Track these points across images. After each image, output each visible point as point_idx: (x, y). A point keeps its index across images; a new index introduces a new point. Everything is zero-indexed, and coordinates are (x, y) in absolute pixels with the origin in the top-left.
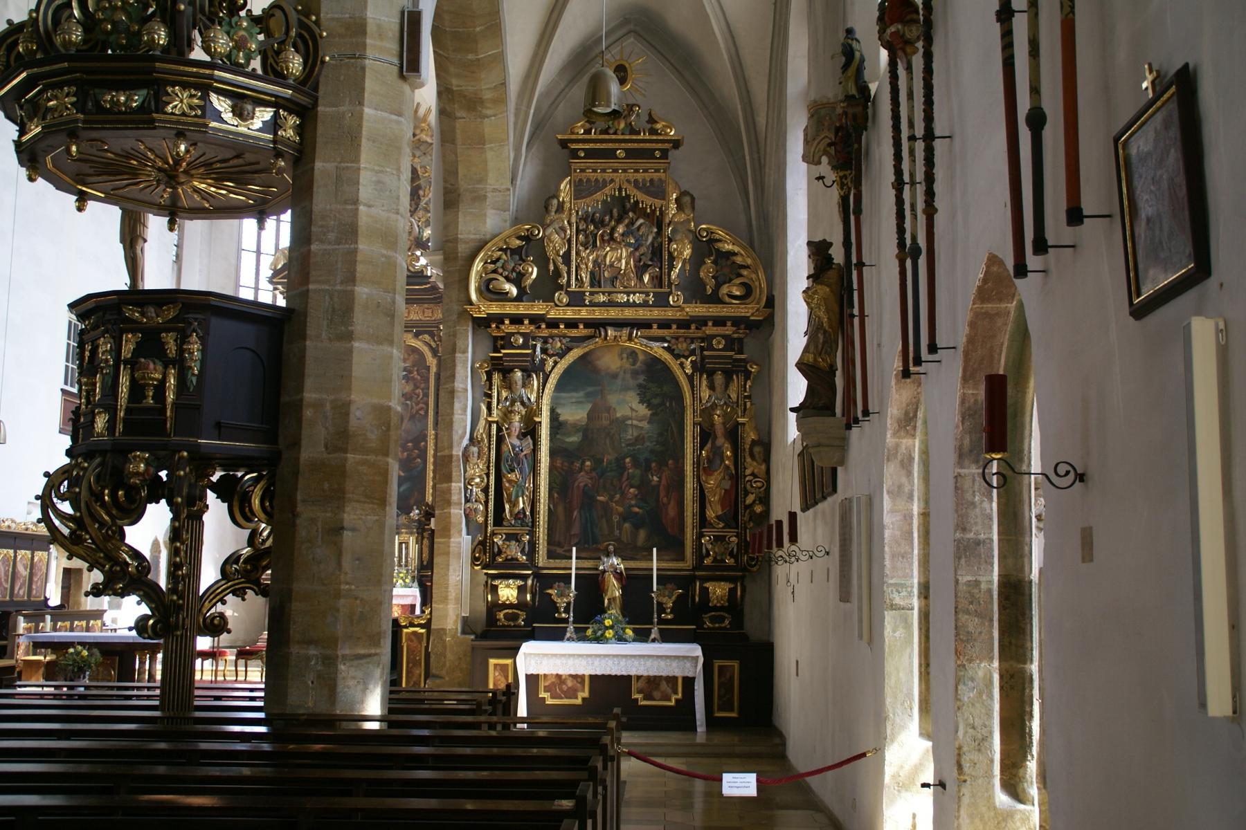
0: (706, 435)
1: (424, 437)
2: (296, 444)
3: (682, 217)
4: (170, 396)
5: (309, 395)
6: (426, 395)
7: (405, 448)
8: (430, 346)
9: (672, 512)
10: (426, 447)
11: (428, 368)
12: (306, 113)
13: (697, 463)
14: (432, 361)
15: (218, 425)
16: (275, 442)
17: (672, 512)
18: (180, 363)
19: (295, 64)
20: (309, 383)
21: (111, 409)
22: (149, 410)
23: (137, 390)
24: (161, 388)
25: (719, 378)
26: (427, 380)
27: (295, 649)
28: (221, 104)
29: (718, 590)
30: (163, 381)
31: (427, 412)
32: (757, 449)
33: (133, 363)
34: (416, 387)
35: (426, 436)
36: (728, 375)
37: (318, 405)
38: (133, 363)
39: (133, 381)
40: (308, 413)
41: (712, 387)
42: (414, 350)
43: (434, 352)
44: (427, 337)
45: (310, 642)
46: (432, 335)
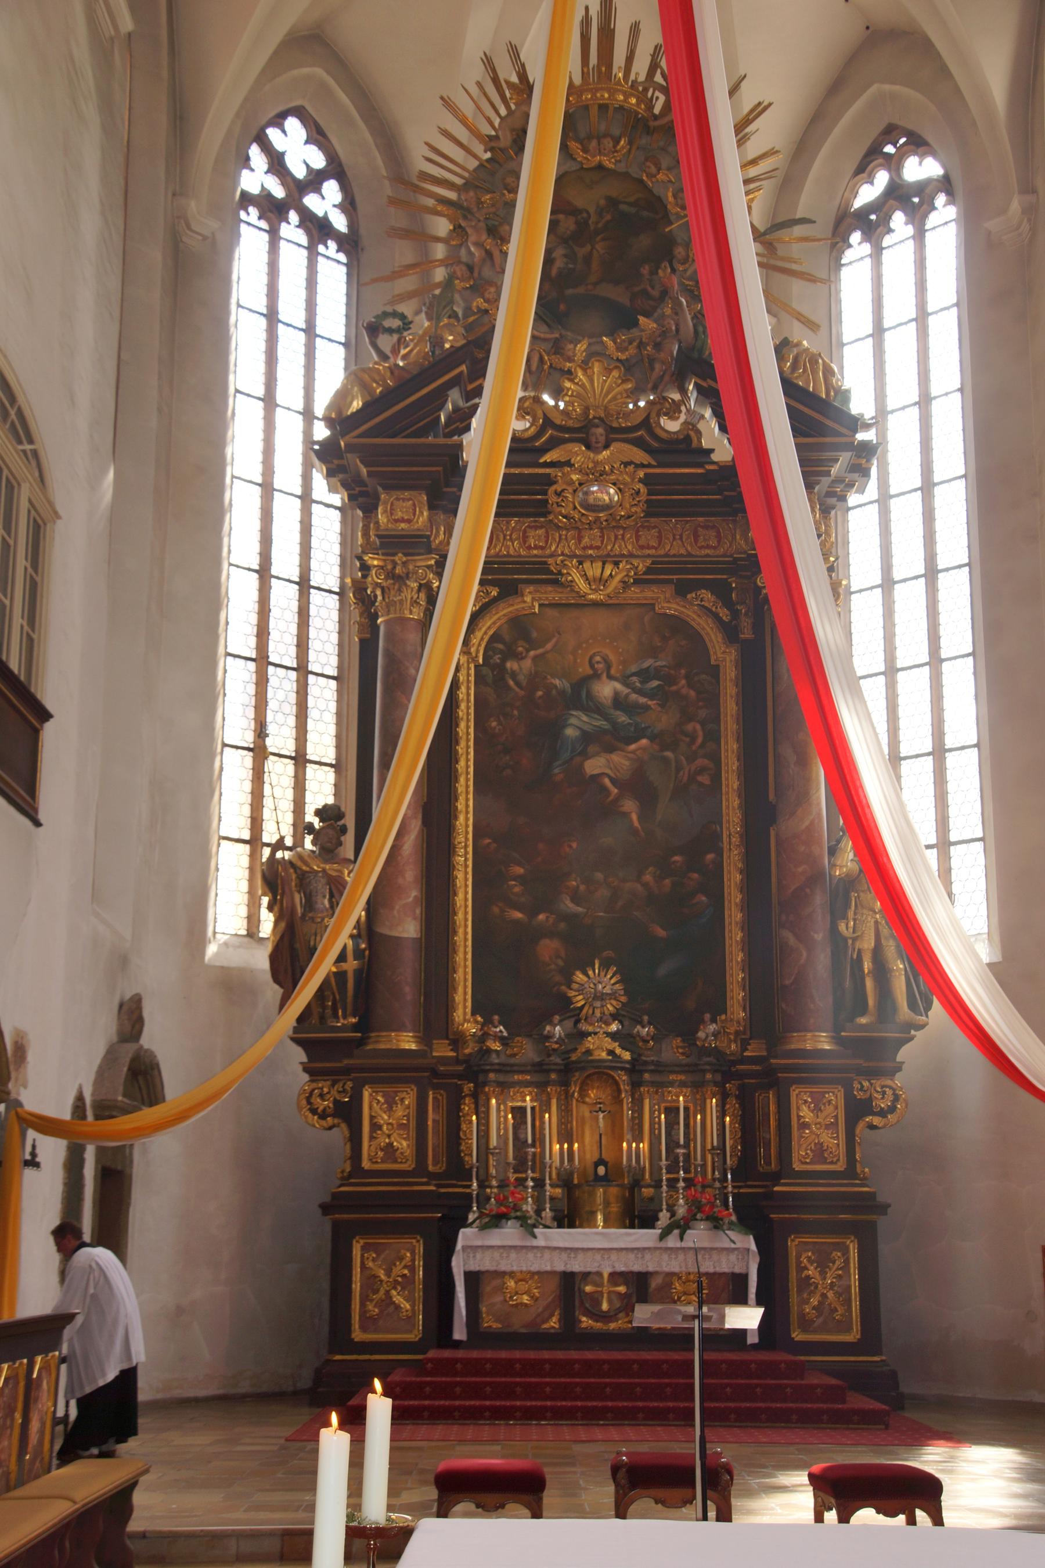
6: (714, 736)
8: (716, 616)
10: (719, 866)
11: (715, 672)
14: (725, 656)
26: (712, 700)
31: (716, 778)
35: (717, 837)
42: (677, 626)
43: (731, 633)
44: (706, 595)
46: (722, 591)
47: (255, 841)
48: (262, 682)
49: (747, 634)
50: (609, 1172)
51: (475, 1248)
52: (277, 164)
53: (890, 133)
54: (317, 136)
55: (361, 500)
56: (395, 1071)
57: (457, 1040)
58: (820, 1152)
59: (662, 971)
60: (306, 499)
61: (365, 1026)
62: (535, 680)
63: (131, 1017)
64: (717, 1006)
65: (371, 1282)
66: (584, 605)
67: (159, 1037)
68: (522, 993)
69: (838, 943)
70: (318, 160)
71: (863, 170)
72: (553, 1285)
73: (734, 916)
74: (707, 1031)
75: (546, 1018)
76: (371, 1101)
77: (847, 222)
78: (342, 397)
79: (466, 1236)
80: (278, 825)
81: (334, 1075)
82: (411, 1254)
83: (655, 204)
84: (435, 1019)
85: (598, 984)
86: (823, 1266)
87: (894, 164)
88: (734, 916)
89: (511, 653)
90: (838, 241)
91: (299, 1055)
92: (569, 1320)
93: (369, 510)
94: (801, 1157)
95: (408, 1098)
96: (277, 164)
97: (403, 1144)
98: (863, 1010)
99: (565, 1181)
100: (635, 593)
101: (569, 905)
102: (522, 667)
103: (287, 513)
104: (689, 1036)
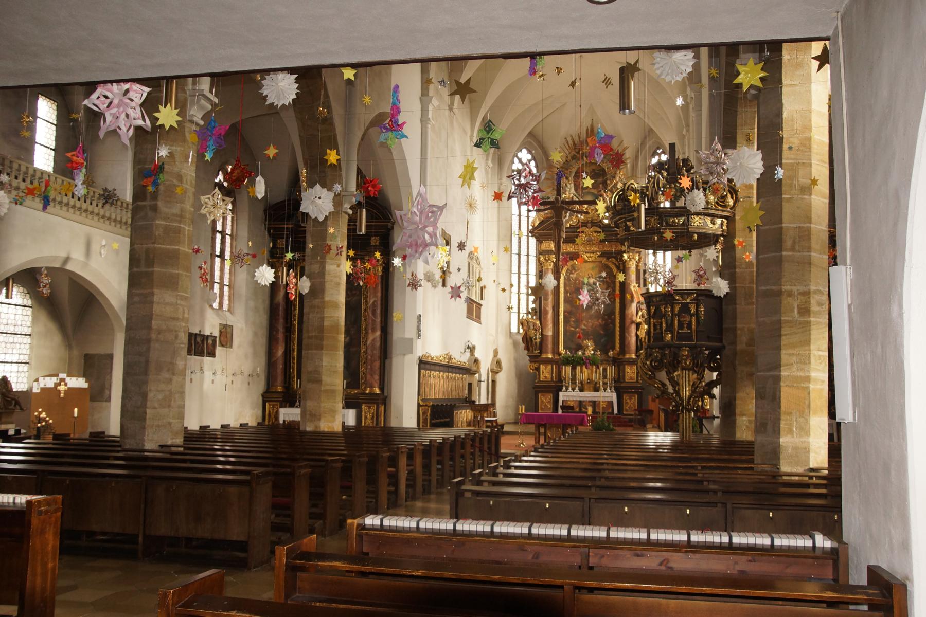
1: (613, 313)
2: (734, 343)
4: (694, 327)
5: (739, 326)
7: (603, 319)
12: (731, 220)
15: (708, 337)
16: (721, 341)
18: (697, 313)
19: (731, 202)
20: (738, 321)
21: (672, 333)
23: (681, 326)
24: (690, 323)
27: (738, 418)
28: (708, 220)
30: (690, 322)
38: (679, 315)
39: (679, 321)
40: (739, 332)
45: (743, 415)
46: (617, 259)
47: (519, 313)
48: (519, 278)
51: (562, 396)
52: (520, 161)
53: (659, 148)
54: (529, 152)
55: (539, 241)
56: (548, 362)
57: (560, 354)
58: (631, 378)
59: (603, 340)
60: (528, 236)
61: (541, 353)
62: (576, 279)
63: (496, 352)
64: (613, 348)
65: (542, 402)
66: (586, 262)
67: (500, 356)
68: (574, 344)
70: (529, 157)
71: (653, 155)
73: (617, 329)
74: (611, 353)
75: (578, 350)
76: (542, 367)
78: (534, 222)
79: (561, 394)
80: (523, 309)
81: (535, 362)
82: (550, 397)
83: (603, 170)
84: (556, 351)
85: (589, 344)
86: (630, 399)
87: (659, 155)
88: (617, 329)
89: (571, 273)
91: (528, 358)
92: (580, 409)
93: (541, 242)
94: (627, 379)
95: (550, 367)
96: (520, 161)
99: (581, 382)
100: (598, 259)
101: (583, 327)
102: (574, 276)
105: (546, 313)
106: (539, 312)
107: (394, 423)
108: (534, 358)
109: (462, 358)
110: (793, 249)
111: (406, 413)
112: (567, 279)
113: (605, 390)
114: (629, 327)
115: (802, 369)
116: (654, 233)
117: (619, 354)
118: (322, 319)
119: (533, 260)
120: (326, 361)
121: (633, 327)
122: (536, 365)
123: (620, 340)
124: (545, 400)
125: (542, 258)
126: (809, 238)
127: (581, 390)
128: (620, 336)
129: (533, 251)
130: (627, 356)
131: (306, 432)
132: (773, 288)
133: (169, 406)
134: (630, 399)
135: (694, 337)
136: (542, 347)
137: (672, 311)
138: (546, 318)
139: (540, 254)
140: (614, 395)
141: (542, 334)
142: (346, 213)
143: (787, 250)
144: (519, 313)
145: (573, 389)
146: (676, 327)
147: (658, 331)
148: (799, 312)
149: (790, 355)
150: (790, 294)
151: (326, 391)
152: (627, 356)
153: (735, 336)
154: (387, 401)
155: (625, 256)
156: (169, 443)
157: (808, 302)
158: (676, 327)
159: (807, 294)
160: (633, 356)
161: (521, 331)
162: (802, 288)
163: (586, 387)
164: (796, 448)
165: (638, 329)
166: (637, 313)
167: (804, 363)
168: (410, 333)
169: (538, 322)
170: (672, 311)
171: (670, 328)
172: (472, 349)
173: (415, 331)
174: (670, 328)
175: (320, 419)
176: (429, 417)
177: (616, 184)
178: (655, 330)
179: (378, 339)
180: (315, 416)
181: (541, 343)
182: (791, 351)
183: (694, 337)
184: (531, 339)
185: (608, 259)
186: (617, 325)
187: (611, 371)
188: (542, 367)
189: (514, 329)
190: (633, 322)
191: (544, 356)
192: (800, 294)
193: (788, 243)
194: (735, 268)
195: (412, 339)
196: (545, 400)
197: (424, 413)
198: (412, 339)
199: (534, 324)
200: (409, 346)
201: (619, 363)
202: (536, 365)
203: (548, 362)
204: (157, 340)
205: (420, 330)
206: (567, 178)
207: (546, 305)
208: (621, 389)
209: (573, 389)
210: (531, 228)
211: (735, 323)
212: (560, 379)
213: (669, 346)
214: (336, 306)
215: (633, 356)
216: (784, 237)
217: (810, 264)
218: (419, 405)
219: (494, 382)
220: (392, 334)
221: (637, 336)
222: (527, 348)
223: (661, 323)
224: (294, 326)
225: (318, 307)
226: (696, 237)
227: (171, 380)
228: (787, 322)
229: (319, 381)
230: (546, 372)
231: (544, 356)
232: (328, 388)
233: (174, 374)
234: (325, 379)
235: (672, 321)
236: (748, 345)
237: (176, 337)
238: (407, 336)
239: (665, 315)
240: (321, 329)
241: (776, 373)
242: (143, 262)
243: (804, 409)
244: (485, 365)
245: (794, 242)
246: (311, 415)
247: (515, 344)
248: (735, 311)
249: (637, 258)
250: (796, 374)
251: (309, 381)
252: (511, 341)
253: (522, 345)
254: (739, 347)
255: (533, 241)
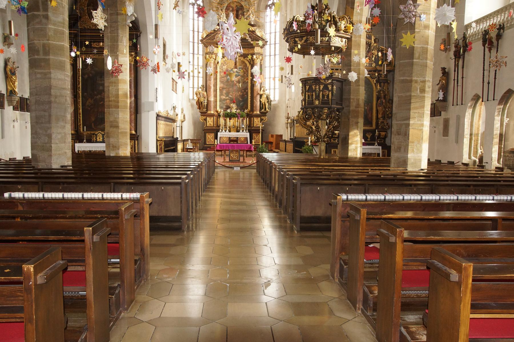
0: (378, 98)
1: (247, 88)
2: (349, 106)
3: (375, 45)
4: (330, 97)
5: (352, 97)
7: (242, 92)
9: (370, 116)
12: (349, 40)
13: (377, 104)
15: (337, 103)
17: (370, 116)
20: (351, 94)
21: (319, 100)
22: (326, 100)
23: (323, 96)
24: (328, 96)
25: (382, 84)
29: (383, 134)
30: (329, 94)
32: (390, 101)
33: (322, 91)
34: (244, 73)
36: (384, 83)
37: (353, 99)
38: (322, 91)
39: (322, 94)
40: (352, 100)
41: (380, 86)
43: (250, 63)
47: (193, 88)
49: (252, 62)
50: (234, 126)
51: (219, 134)
57: (217, 112)
60: (198, 43)
61: (207, 110)
64: (247, 108)
65: (209, 138)
69: (260, 101)
72: (228, 139)
74: (246, 111)
76: (208, 119)
77: (267, 6)
79: (219, 133)
80: (196, 86)
83: (242, 6)
85: (234, 106)
86: (257, 136)
90: (266, 8)
93: (207, 47)
95: (212, 118)
97: (212, 124)
98: (263, 109)
99: (229, 127)
101: (230, 96)
103: (196, 45)
104: (244, 111)
105: (210, 88)
106: (206, 87)
107: (144, 151)
108: (203, 114)
109: (171, 114)
110: (419, 58)
111: (150, 145)
112: (221, 67)
113: (243, 131)
114: (256, 96)
115: (420, 120)
116: (312, 46)
117: (250, 112)
118: (118, 90)
119: (201, 58)
120: (121, 115)
121: (258, 96)
122: (204, 117)
123: (251, 103)
124: (210, 137)
125: (207, 57)
126: (427, 53)
127: (230, 131)
128: (251, 101)
129: (201, 52)
130: (255, 113)
131: (110, 157)
132: (407, 78)
133: (65, 142)
134: (257, 136)
135: (330, 103)
136: (207, 107)
137: (319, 88)
138: (210, 91)
139: (206, 54)
140: (248, 134)
141: (208, 100)
142: (128, 25)
143: (416, 59)
144: (193, 88)
145: (225, 131)
146: (321, 97)
147: (311, 99)
148: (420, 91)
149: (415, 113)
150: (416, 82)
151: (122, 133)
152: (255, 113)
153: (350, 102)
154: (139, 137)
155: (255, 57)
156: (66, 164)
157: (424, 86)
158: (321, 97)
159: (424, 82)
160: (258, 113)
161: (195, 98)
162: (422, 79)
163: (232, 129)
164: (415, 160)
165: (261, 98)
166: (261, 89)
167: (421, 117)
168: (151, 99)
169: (205, 93)
170: (319, 88)
171: (317, 97)
172: (174, 108)
173: (155, 97)
174: (317, 97)
175: (119, 149)
176: (163, 147)
177: (250, 15)
178: (308, 98)
179: (133, 102)
180: (116, 147)
181: (207, 105)
182: (415, 111)
183: (330, 103)
184: (202, 103)
185: (244, 58)
186: (249, 95)
187: (246, 121)
188: (208, 119)
189: (191, 97)
190: (258, 94)
191: (209, 112)
192: (421, 82)
193: (416, 55)
194: (351, 66)
195: (153, 102)
196: (210, 137)
197: (160, 145)
198: (153, 102)
199: (203, 94)
200: (151, 106)
201: (250, 116)
202: (204, 117)
203: (212, 115)
204: (56, 102)
205: (157, 97)
206: (221, 10)
207: (210, 83)
208: (252, 131)
209: (225, 131)
210: (200, 38)
211: (350, 96)
212: (218, 126)
213: (317, 107)
214: (125, 82)
215: (258, 113)
216: (415, 52)
217: (426, 66)
218: (157, 140)
219: (181, 127)
220: (141, 99)
221: (260, 101)
222: (199, 108)
223: (313, 95)
224: (79, 94)
225: (115, 83)
226: (333, 48)
227: (65, 126)
228: (414, 96)
229: (117, 127)
230: (210, 122)
231: (209, 112)
232: (122, 130)
233: (66, 123)
234: (121, 125)
235: (319, 94)
236: (356, 107)
237: (66, 100)
238: (150, 100)
239: (315, 91)
240: (117, 96)
241: (407, 122)
242: (41, 52)
243: (420, 140)
244: (180, 118)
245: (419, 55)
246: (113, 147)
247: (192, 106)
248: (350, 90)
249: (261, 58)
250: (417, 122)
251: (111, 127)
252: (190, 104)
253: (196, 106)
254: (351, 108)
255: (201, 46)
